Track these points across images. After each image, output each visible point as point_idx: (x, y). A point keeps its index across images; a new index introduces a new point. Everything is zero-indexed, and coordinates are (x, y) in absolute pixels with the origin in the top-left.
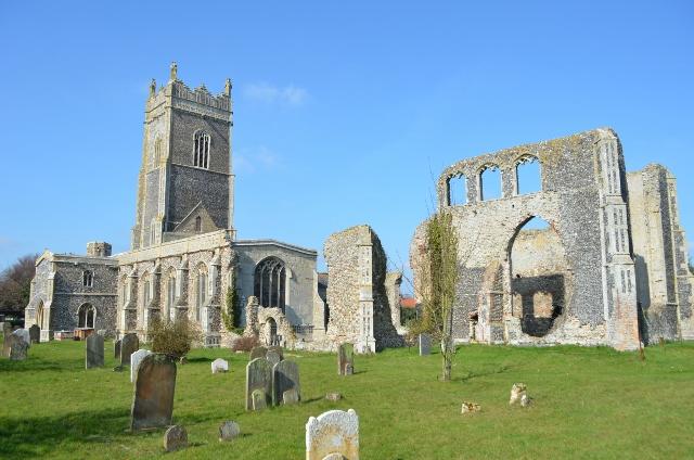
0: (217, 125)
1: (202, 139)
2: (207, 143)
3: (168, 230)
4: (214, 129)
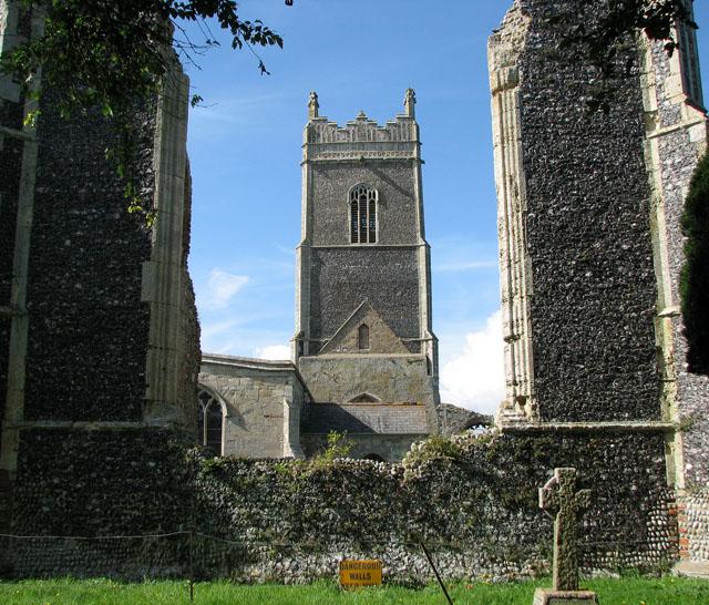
0: (389, 172)
1: (363, 198)
2: (372, 202)
3: (310, 353)
4: (384, 177)
